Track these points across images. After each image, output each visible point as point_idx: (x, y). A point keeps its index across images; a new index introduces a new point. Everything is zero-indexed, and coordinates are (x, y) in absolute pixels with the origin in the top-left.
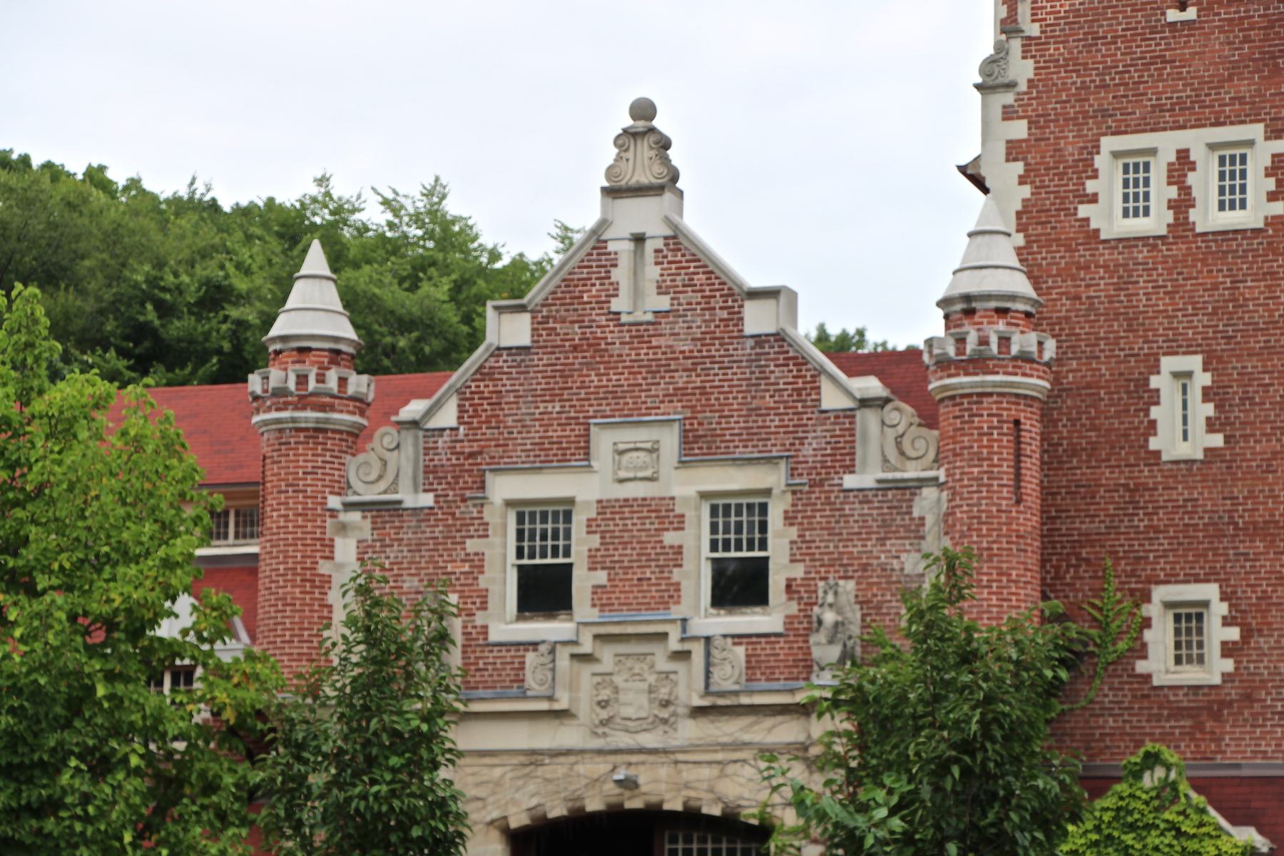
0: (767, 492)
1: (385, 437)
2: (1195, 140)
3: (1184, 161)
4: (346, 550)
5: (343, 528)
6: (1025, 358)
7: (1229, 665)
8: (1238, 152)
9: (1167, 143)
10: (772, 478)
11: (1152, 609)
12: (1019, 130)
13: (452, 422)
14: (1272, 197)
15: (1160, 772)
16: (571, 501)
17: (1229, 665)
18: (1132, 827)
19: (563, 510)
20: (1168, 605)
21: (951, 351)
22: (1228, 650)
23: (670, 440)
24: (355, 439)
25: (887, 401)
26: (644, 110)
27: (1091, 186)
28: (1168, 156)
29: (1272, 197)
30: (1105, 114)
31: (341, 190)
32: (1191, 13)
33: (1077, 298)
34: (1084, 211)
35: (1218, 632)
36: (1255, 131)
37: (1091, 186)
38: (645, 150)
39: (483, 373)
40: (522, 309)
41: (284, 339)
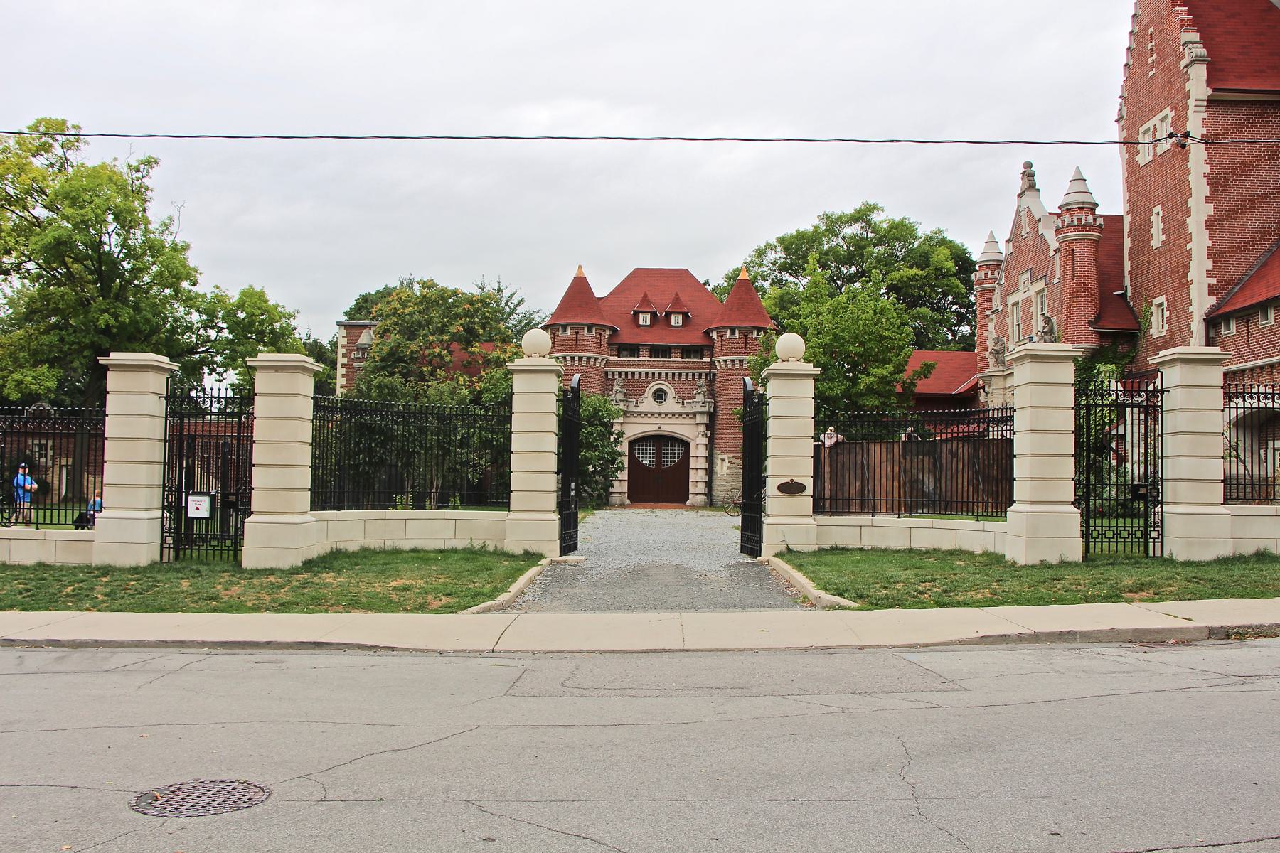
6: (1087, 224)
9: (1150, 124)
28: (1152, 129)
36: (1167, 111)
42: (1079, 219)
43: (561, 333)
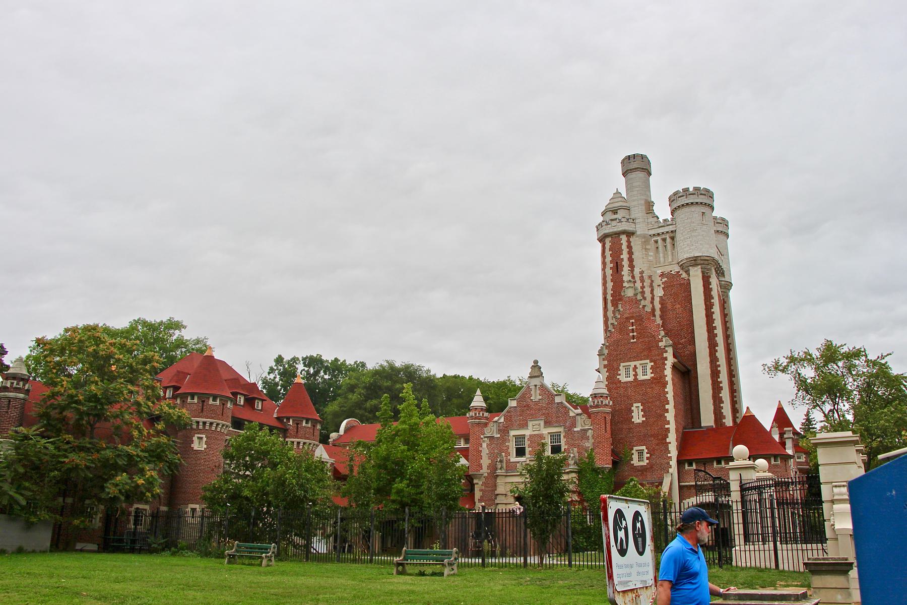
0: (560, 432)
1: (491, 424)
2: (637, 363)
3: (635, 367)
4: (484, 445)
5: (484, 441)
7: (648, 461)
8: (645, 365)
9: (632, 364)
10: (561, 429)
11: (634, 451)
12: (606, 363)
13: (503, 421)
14: (651, 373)
15: (633, 482)
16: (525, 435)
17: (648, 461)
18: (628, 493)
19: (523, 437)
20: (637, 451)
21: (592, 404)
22: (647, 458)
23: (542, 423)
24: (486, 425)
25: (582, 414)
26: (536, 362)
27: (619, 372)
29: (651, 373)
30: (621, 359)
31: (512, 378)
32: (635, 340)
33: (618, 393)
34: (618, 377)
35: (646, 455)
37: (619, 372)
38: (536, 369)
39: (508, 412)
40: (515, 399)
41: (473, 407)
42: (602, 402)
43: (189, 400)
